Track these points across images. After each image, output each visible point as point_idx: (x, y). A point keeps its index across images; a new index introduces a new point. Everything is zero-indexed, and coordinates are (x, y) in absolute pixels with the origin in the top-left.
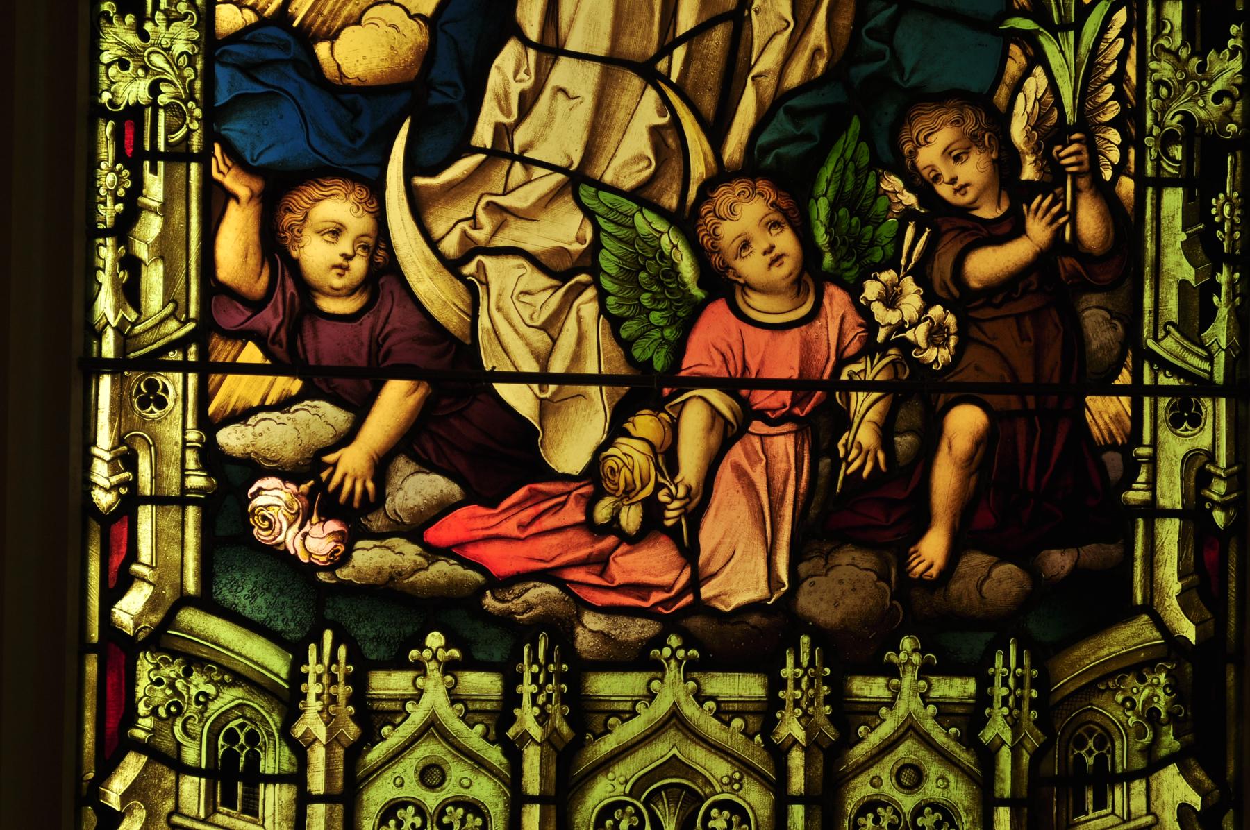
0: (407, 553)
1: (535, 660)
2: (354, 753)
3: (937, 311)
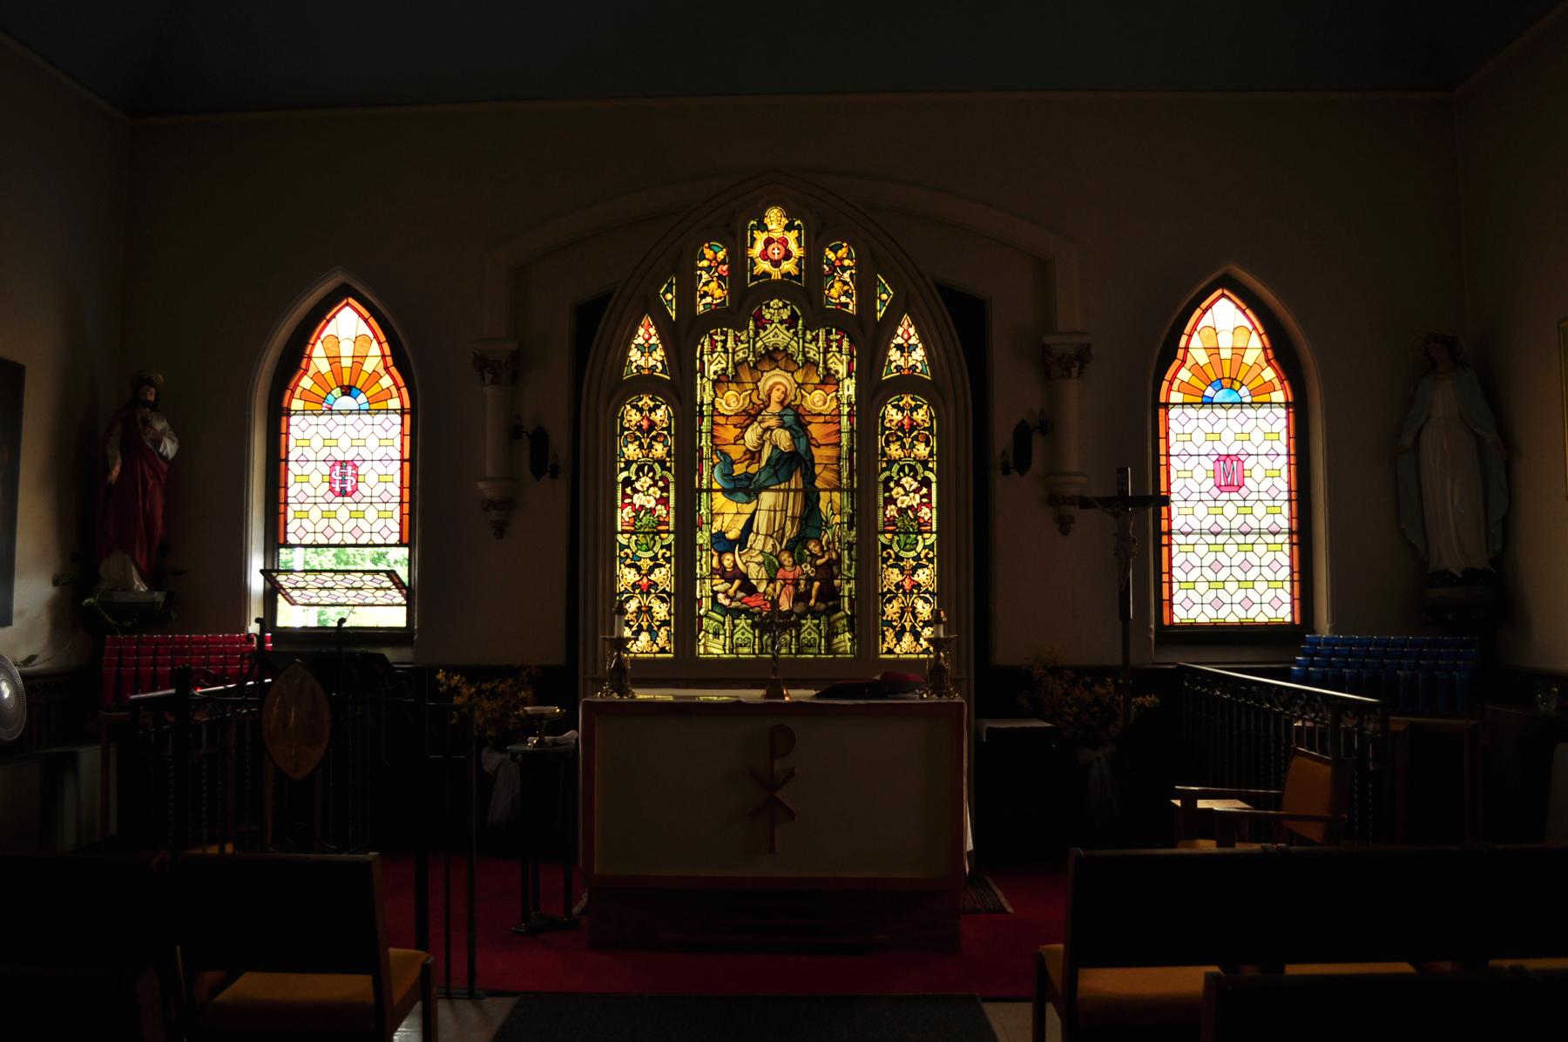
0: (739, 604)
2: (733, 631)
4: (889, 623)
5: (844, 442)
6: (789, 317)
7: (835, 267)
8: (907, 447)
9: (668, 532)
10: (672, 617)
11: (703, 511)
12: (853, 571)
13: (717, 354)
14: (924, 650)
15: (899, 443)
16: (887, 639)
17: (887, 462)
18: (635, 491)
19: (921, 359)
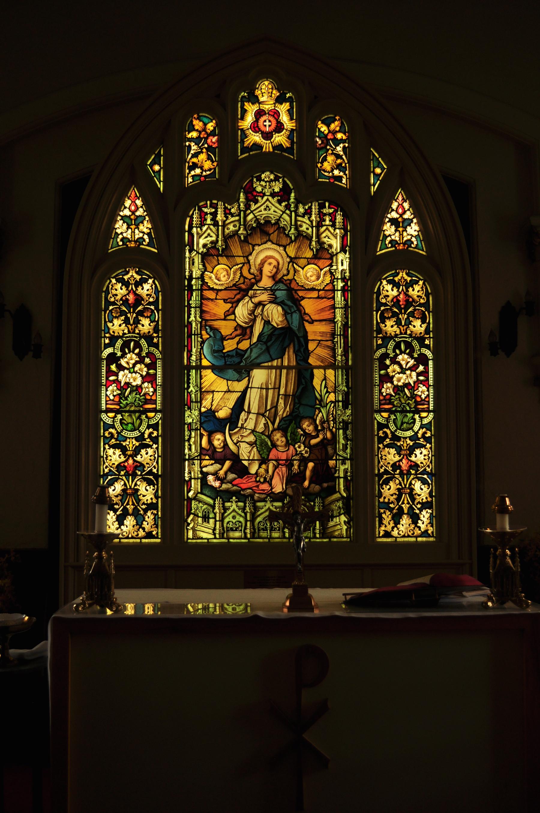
0: (230, 486)
1: (248, 501)
2: (223, 514)
3: (306, 449)
4: (386, 506)
5: (339, 318)
6: (281, 189)
7: (328, 140)
8: (403, 323)
9: (155, 410)
10: (160, 500)
11: (191, 388)
12: (348, 451)
13: (206, 227)
14: (423, 533)
15: (394, 319)
16: (384, 522)
17: (383, 339)
18: (121, 368)
19: (416, 233)
